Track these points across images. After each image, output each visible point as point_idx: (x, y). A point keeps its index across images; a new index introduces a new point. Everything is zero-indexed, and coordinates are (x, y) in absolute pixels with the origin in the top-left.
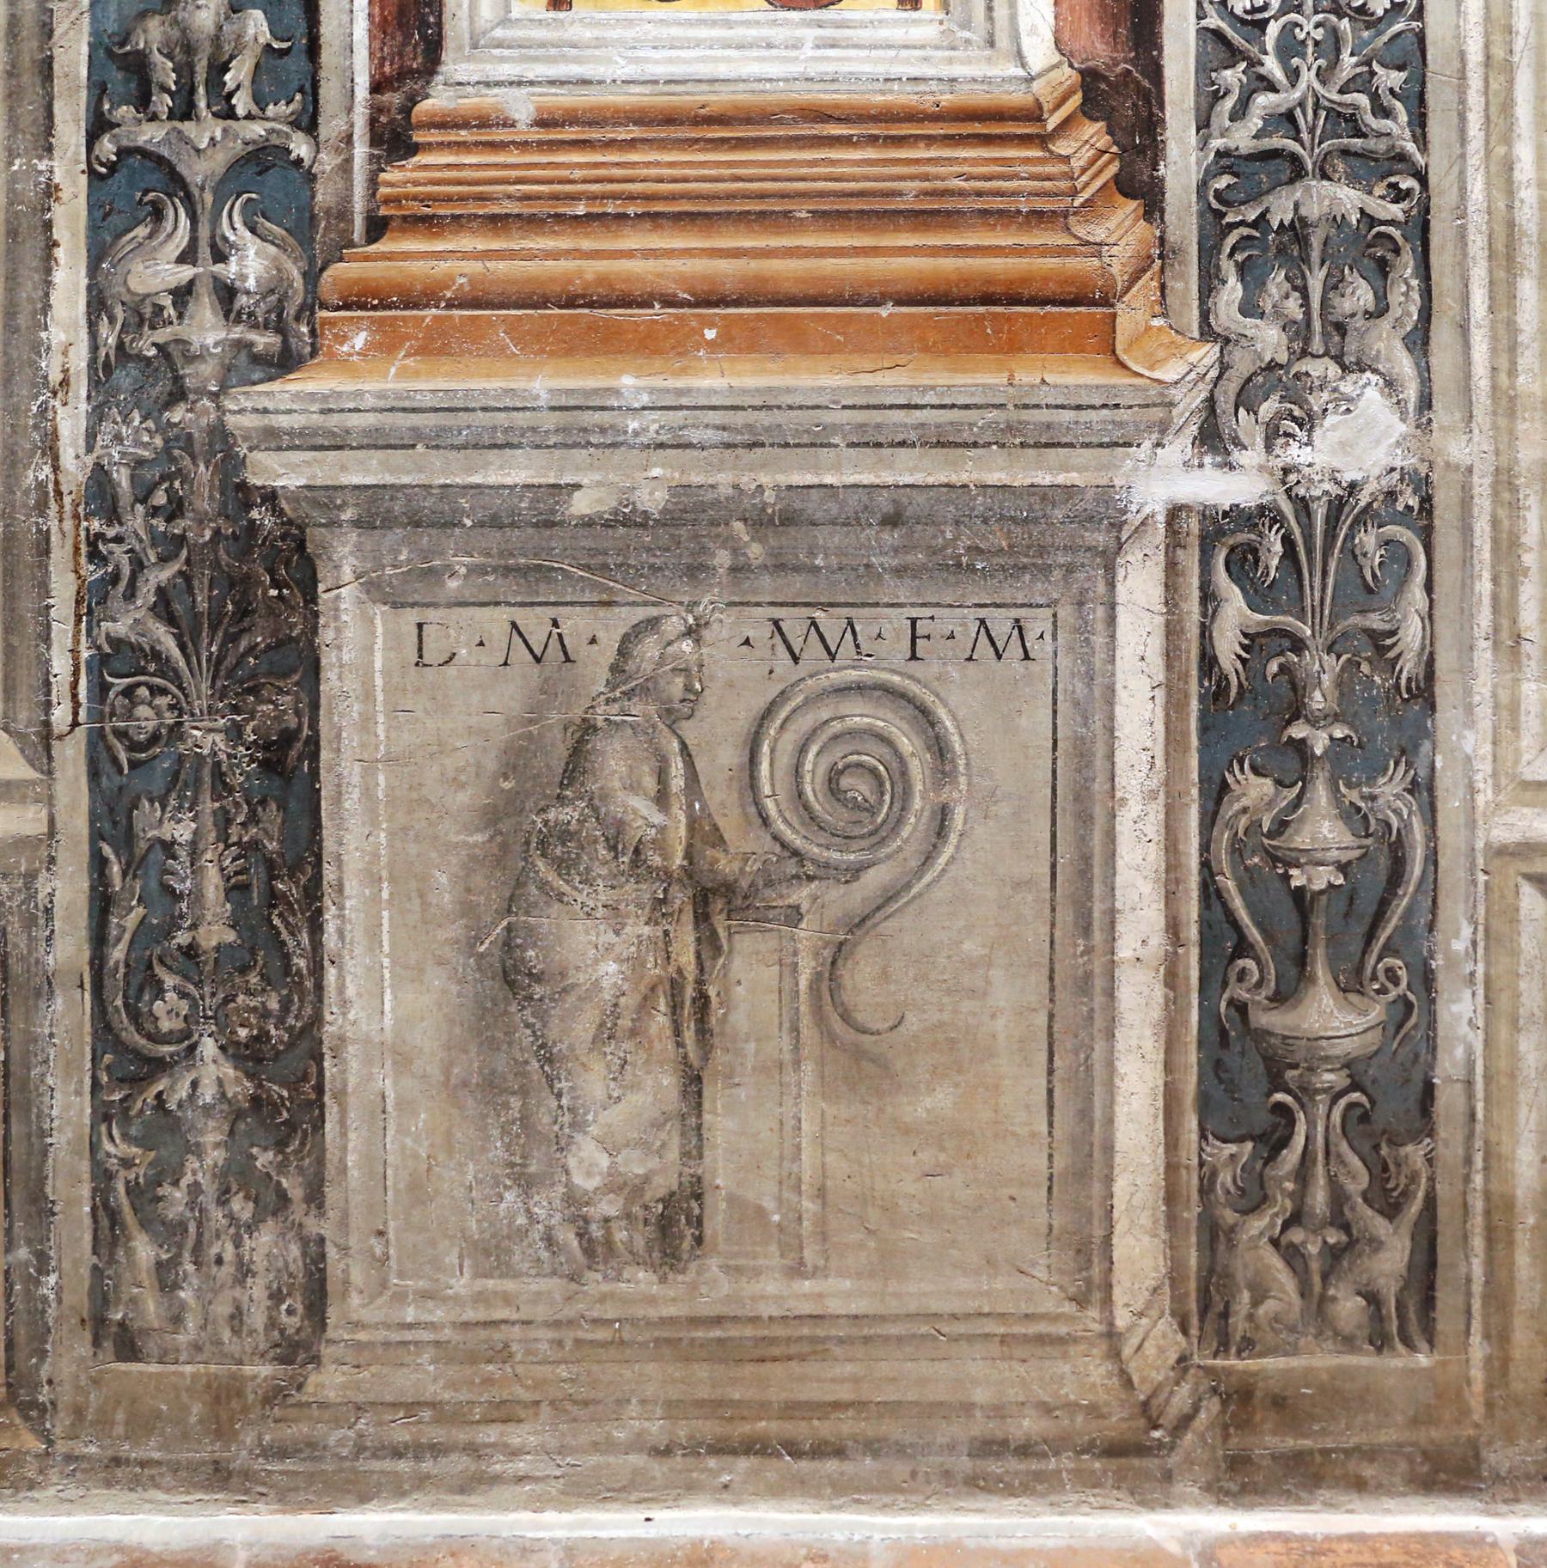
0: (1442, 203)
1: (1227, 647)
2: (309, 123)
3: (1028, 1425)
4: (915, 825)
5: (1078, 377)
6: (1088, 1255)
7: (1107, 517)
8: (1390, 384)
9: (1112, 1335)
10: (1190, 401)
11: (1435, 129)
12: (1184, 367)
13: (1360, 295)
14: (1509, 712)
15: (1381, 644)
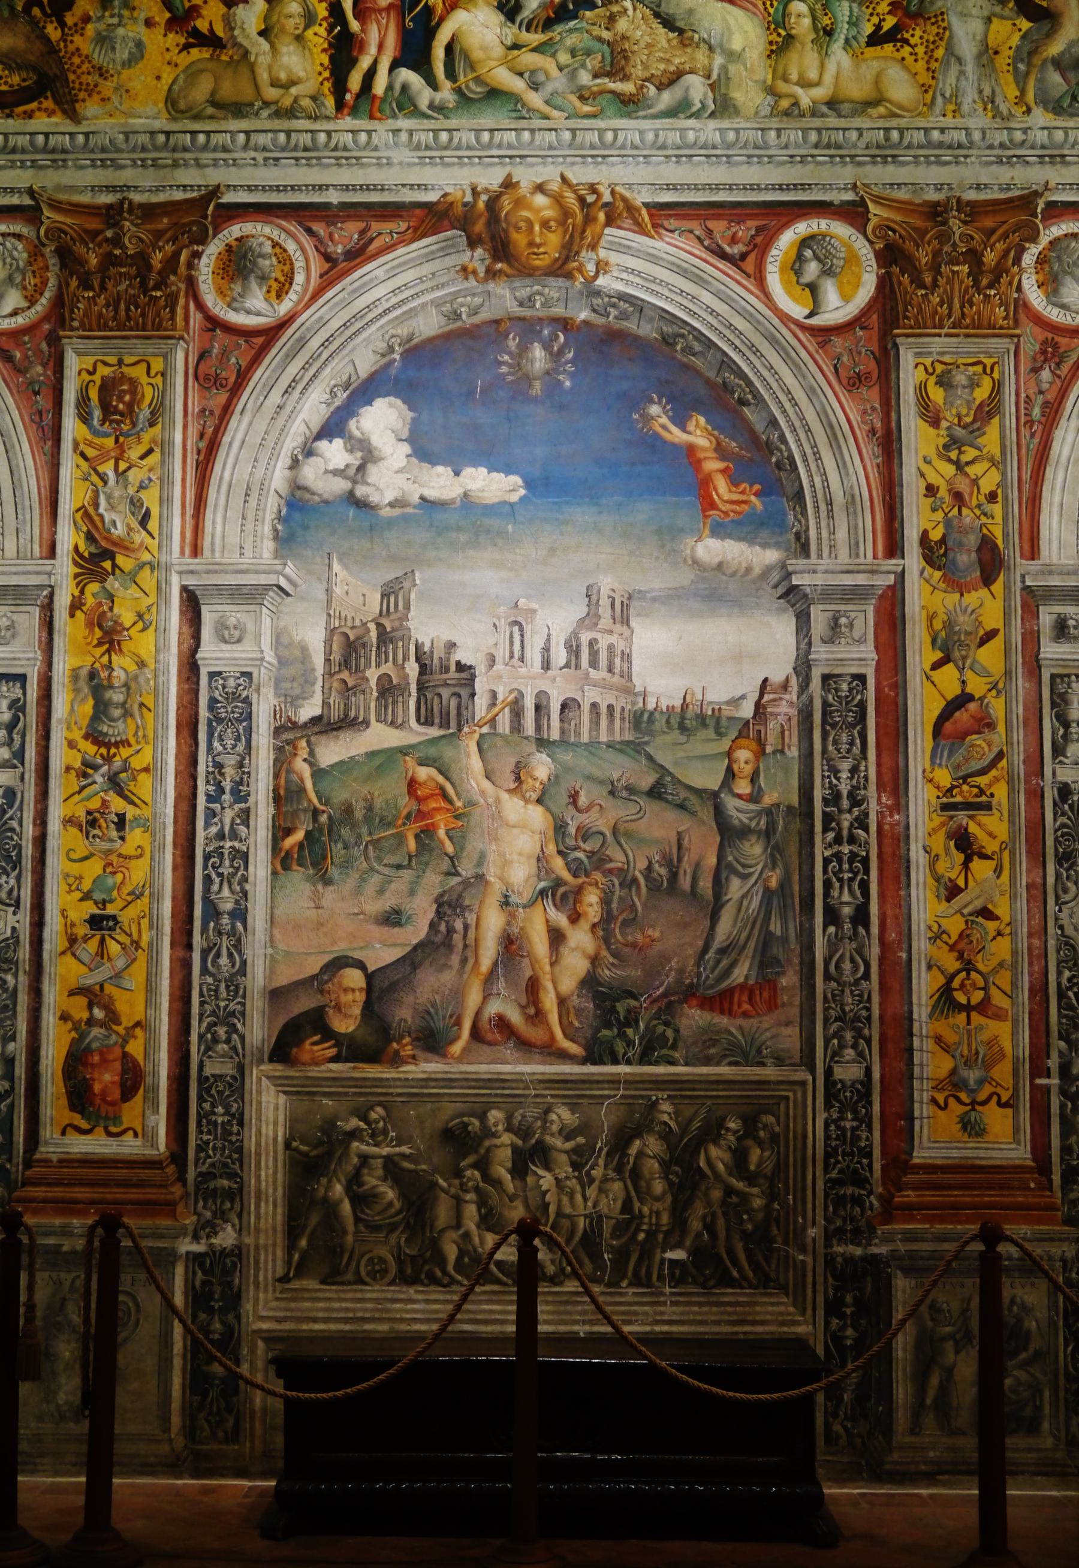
0: (246, 1184)
1: (198, 1284)
2: (10, 1160)
3: (152, 1459)
4: (132, 1323)
5: (166, 1222)
6: (165, 1420)
7: (169, 1257)
8: (233, 1226)
9: (170, 1440)
10: (191, 1228)
11: (245, 1167)
12: (190, 1221)
13: (228, 1205)
14: (256, 1300)
15: (230, 1284)
